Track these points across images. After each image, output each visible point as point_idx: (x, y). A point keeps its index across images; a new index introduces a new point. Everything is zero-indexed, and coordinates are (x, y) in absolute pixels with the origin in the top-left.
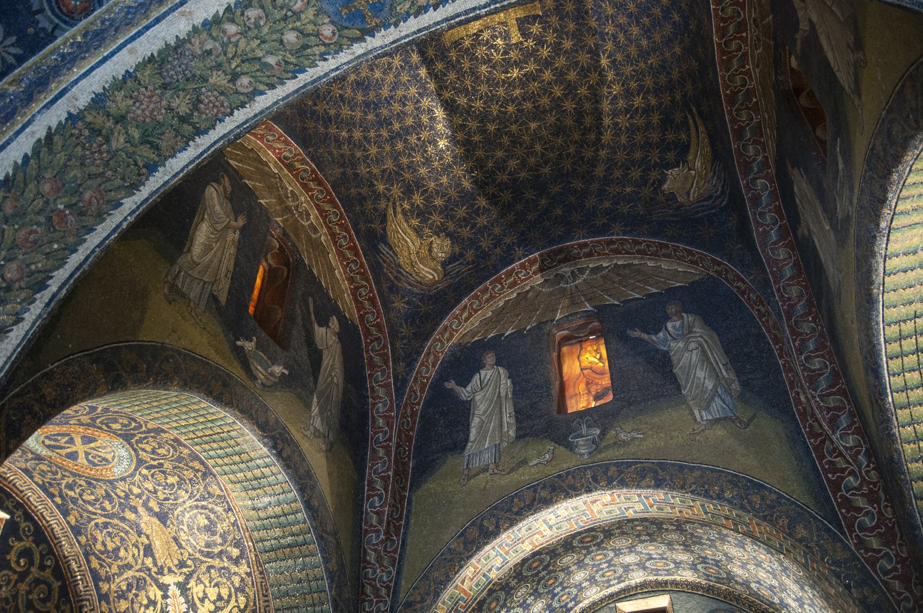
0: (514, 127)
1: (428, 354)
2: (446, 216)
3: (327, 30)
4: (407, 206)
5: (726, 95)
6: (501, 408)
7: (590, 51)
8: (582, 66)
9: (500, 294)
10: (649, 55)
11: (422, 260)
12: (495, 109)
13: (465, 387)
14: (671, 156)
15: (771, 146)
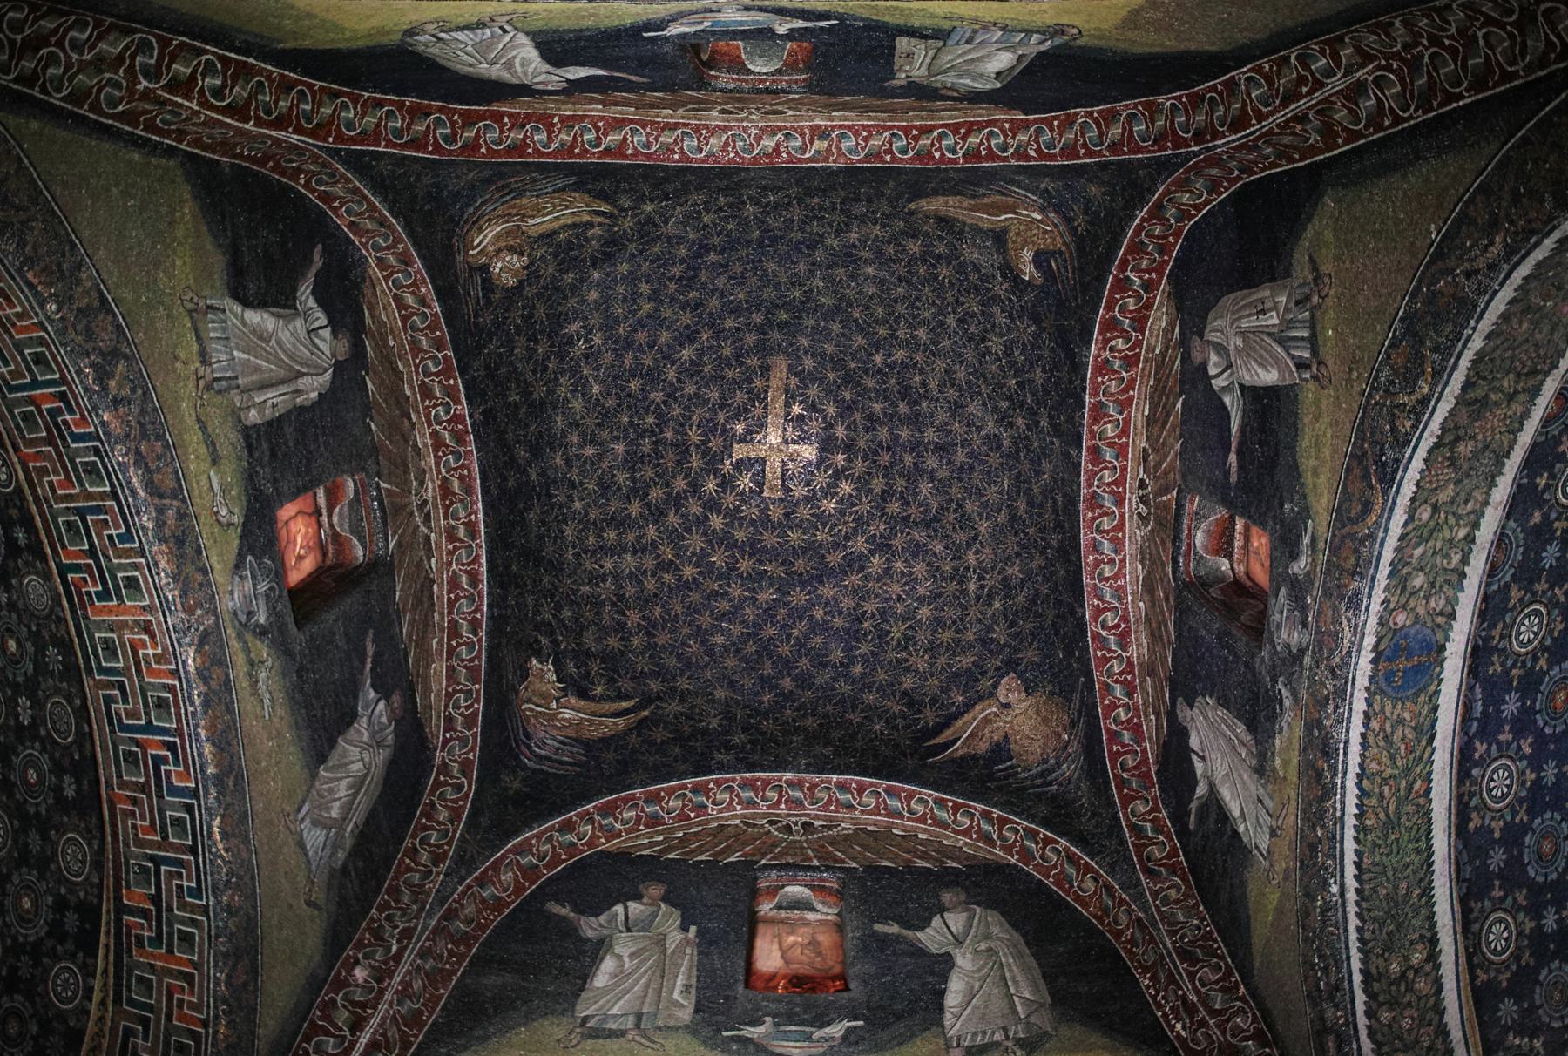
0: (626, 420)
1: (383, 223)
2: (546, 288)
3: (1401, 619)
4: (597, 231)
5: (708, 782)
6: (283, 382)
7: (704, 554)
8: (684, 538)
9: (417, 366)
10: (702, 643)
11: (508, 232)
12: (657, 396)
13: (313, 293)
14: (571, 667)
15: (644, 843)
